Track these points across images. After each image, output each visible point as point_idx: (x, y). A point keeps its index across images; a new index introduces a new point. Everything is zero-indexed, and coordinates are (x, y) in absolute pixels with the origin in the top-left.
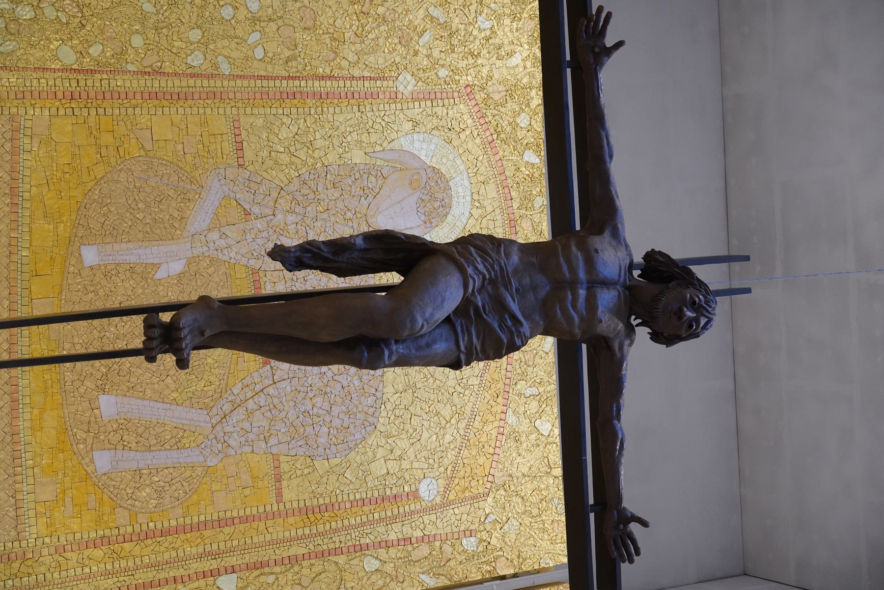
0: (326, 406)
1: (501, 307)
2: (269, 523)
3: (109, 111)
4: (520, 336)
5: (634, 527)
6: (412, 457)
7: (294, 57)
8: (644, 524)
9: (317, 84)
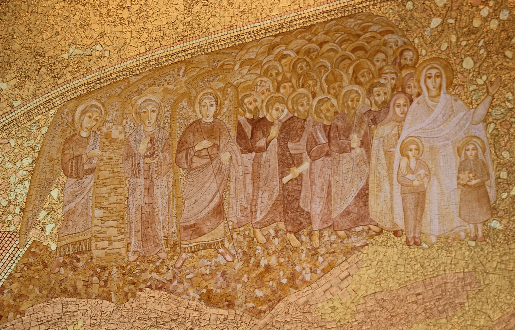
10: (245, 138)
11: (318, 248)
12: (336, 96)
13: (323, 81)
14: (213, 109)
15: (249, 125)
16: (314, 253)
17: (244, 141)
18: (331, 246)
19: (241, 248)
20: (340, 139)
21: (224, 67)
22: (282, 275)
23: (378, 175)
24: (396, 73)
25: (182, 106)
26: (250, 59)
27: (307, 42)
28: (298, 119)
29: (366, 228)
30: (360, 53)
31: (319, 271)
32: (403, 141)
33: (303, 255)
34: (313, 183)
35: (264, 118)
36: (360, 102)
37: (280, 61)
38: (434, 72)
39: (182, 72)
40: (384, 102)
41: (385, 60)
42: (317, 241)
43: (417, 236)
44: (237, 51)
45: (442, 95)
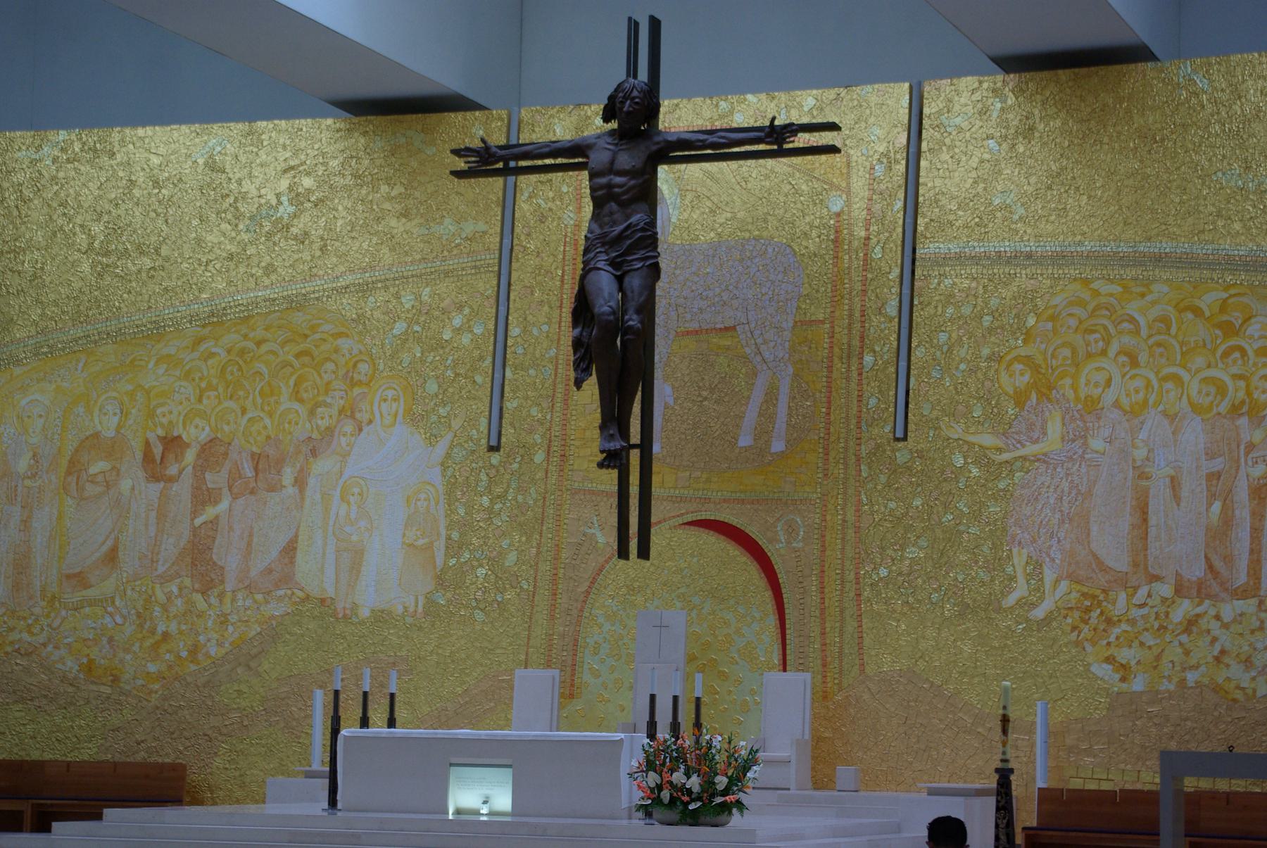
0: (768, 284)
1: (620, 237)
2: (837, 329)
3: (573, 432)
4: (638, 224)
5: (777, 123)
6: (812, 217)
7: (549, 302)
8: (774, 119)
9: (566, 286)
10: (153, 461)
11: (229, 614)
12: (271, 415)
13: (257, 392)
14: (116, 419)
15: (160, 445)
16: (223, 621)
17: (151, 465)
18: (245, 612)
19: (134, 608)
20: (270, 473)
21: (136, 363)
22: (181, 647)
23: (311, 525)
24: (346, 391)
25: (77, 412)
26: (168, 356)
27: (242, 339)
28: (221, 441)
29: (289, 592)
30: (306, 359)
31: (227, 645)
32: (345, 482)
33: (210, 624)
34: (231, 528)
35: (179, 437)
36: (299, 426)
37: (205, 360)
38: (390, 393)
39: (81, 365)
40: (327, 428)
41: (334, 372)
42: (229, 605)
43: (347, 606)
44: (153, 343)
45: (397, 425)
